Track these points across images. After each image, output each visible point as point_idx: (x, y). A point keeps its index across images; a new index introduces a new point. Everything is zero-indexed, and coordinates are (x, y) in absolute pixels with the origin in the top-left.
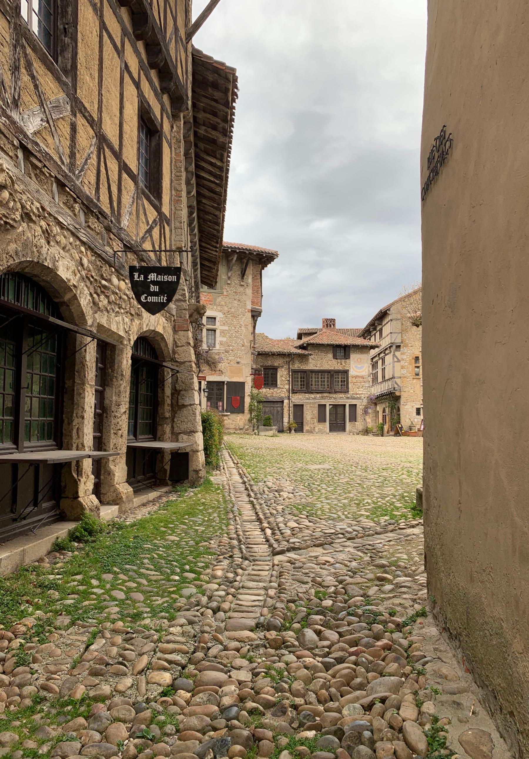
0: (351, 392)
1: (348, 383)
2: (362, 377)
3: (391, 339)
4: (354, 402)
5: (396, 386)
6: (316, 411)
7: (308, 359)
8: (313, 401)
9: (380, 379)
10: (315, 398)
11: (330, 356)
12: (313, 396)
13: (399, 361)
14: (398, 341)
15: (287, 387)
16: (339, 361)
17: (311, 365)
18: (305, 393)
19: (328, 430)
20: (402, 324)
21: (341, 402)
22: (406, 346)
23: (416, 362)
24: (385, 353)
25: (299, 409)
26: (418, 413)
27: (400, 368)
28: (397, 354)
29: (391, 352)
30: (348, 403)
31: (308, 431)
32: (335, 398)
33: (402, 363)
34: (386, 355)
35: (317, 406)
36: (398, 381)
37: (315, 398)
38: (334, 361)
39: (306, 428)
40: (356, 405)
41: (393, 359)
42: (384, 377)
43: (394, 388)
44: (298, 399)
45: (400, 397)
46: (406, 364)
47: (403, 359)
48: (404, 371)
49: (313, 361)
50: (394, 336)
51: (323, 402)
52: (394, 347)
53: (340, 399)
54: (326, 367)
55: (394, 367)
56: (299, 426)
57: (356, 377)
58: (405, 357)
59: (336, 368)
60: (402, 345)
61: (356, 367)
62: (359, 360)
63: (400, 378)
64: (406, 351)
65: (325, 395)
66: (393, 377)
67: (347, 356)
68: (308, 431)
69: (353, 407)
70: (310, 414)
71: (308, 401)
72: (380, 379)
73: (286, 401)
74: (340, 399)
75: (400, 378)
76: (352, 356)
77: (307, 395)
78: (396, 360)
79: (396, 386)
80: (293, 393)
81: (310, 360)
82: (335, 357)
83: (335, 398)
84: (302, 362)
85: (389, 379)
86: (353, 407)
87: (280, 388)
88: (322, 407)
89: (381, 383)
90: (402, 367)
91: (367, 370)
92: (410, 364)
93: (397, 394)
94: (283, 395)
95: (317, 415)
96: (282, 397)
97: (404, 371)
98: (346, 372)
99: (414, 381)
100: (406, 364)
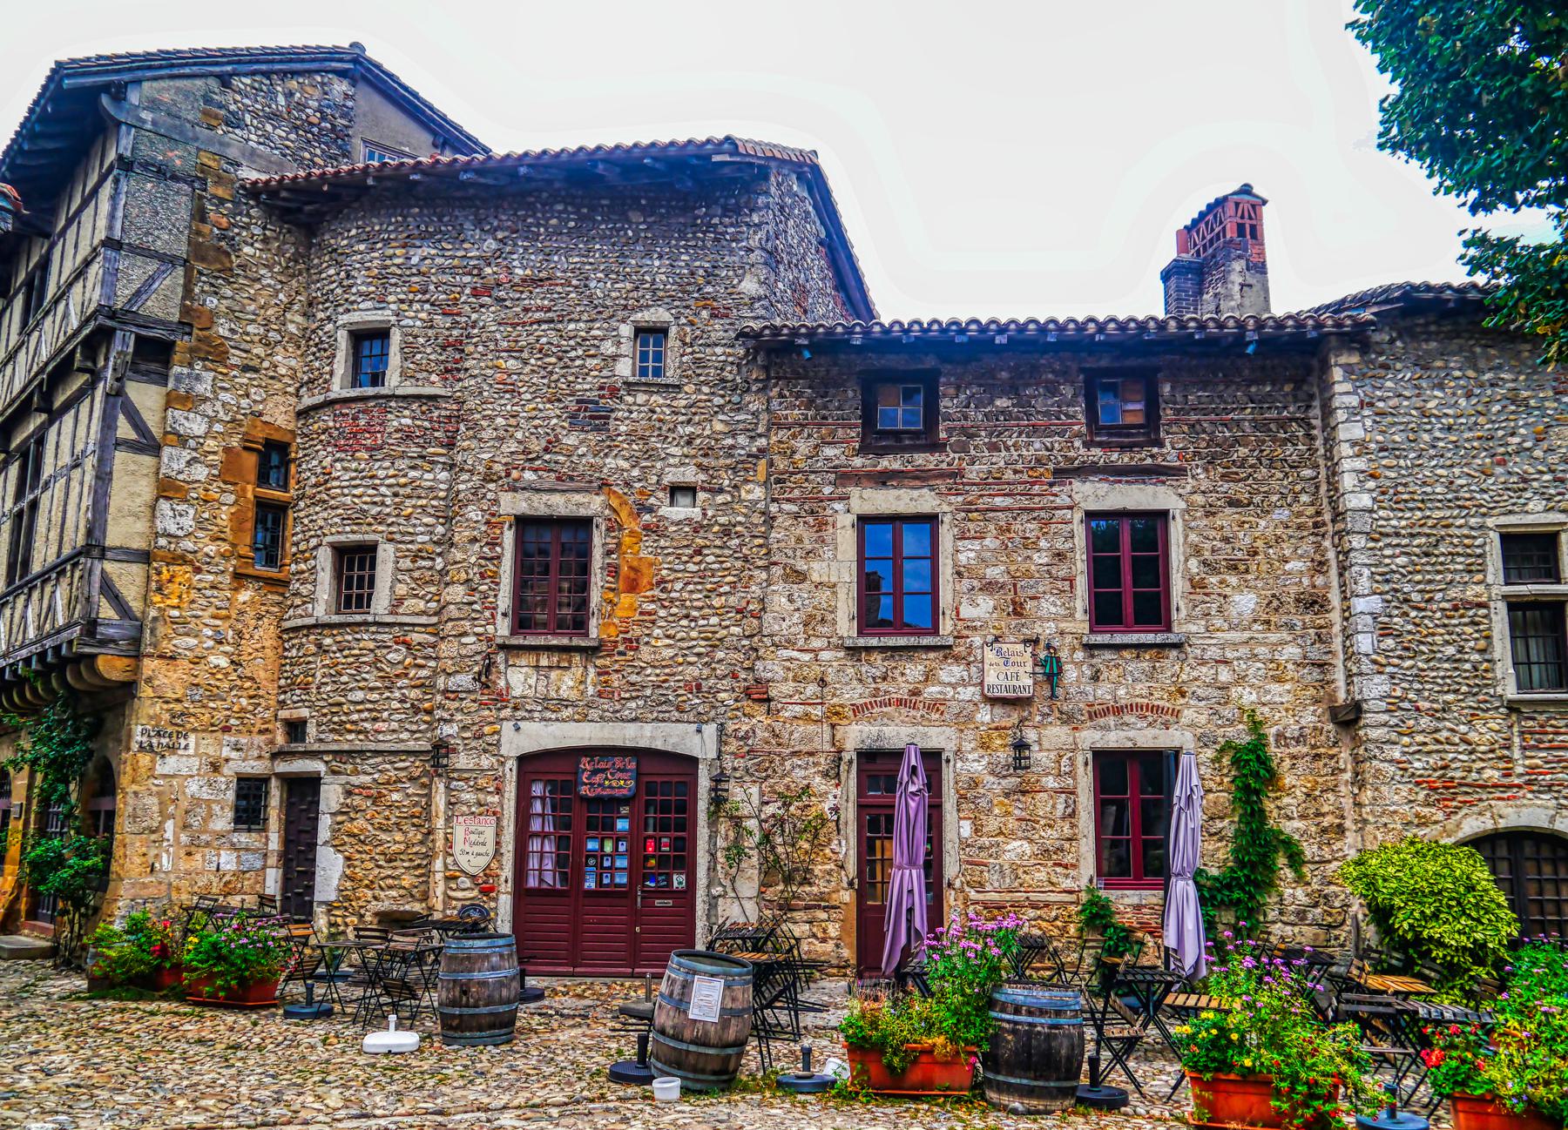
3: (111, 278)
5: (107, 611)
13: (148, 445)
14: (163, 303)
20: (200, 215)
22: (214, 354)
23: (262, 479)
24: (46, 407)
26: (249, 811)
27: (146, 489)
28: (146, 397)
29: (91, 386)
33: (174, 460)
34: (55, 416)
36: (128, 580)
41: (108, 423)
43: (91, 626)
45: (127, 691)
46: (200, 472)
47: (182, 440)
48: (176, 519)
50: (136, 272)
52: (123, 345)
55: (103, 477)
58: (195, 426)
60: (183, 343)
63: (145, 557)
64: (203, 388)
66: (94, 547)
75: (145, 557)
78: (124, 430)
79: (107, 611)
85: (57, 570)
90: (167, 489)
92: (228, 473)
93: (111, 667)
97: (176, 519)
99: (244, 596)
100: (200, 472)
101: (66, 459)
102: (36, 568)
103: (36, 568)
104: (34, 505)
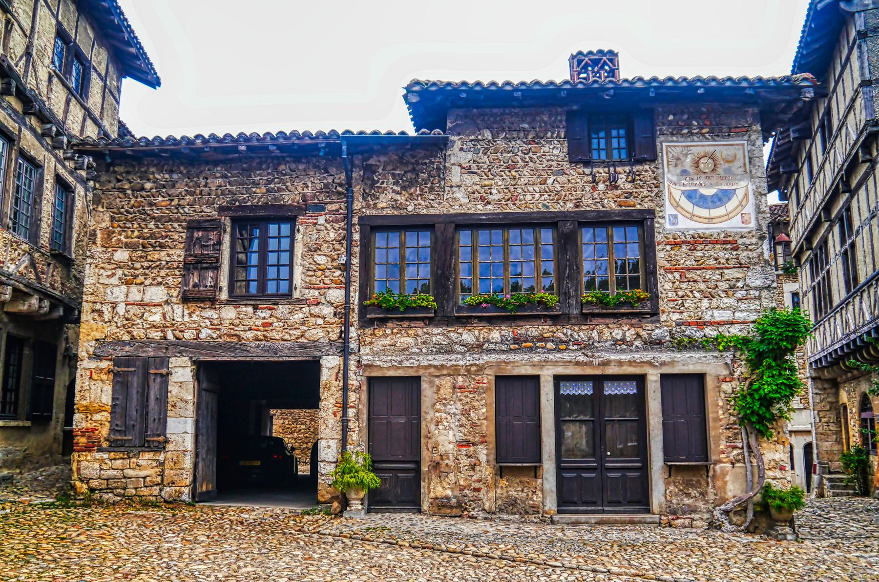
0: (670, 317)
1: (651, 273)
2: (729, 242)
4: (688, 362)
6: (484, 410)
7: (442, 172)
8: (469, 359)
9: (839, 292)
10: (478, 348)
11: (555, 150)
12: (468, 336)
15: (337, 295)
16: (601, 172)
17: (460, 195)
18: (429, 322)
19: (551, 504)
21: (619, 361)
25: (396, 400)
30: (654, 366)
31: (442, 507)
32: (585, 347)
34: (853, 193)
35: (488, 379)
37: (478, 348)
38: (577, 176)
39: (435, 489)
40: (701, 378)
42: (851, 278)
44: (391, 350)
49: (469, 179)
51: (521, 364)
53: (613, 349)
54: (533, 200)
56: (397, 478)
57: (696, 242)
59: (589, 204)
61: (690, 196)
62: (706, 165)
65: (533, 330)
67: (641, 152)
68: (442, 507)
69: (687, 389)
70: (453, 427)
71: (440, 360)
72: (839, 292)
73: (330, 363)
74: (613, 349)
76: (669, 148)
77: (437, 334)
80: (366, 322)
81: (455, 176)
82: (580, 155)
83: (585, 347)
84: (412, 183)
86: (687, 389)
87: (302, 301)
88: (514, 390)
89: (845, 303)
91: (750, 209)
94: (318, 334)
95: (488, 428)
96: (313, 344)
98: (641, 222)
101: (866, 214)
102: (862, 280)
103: (862, 280)
104: (853, 246)
